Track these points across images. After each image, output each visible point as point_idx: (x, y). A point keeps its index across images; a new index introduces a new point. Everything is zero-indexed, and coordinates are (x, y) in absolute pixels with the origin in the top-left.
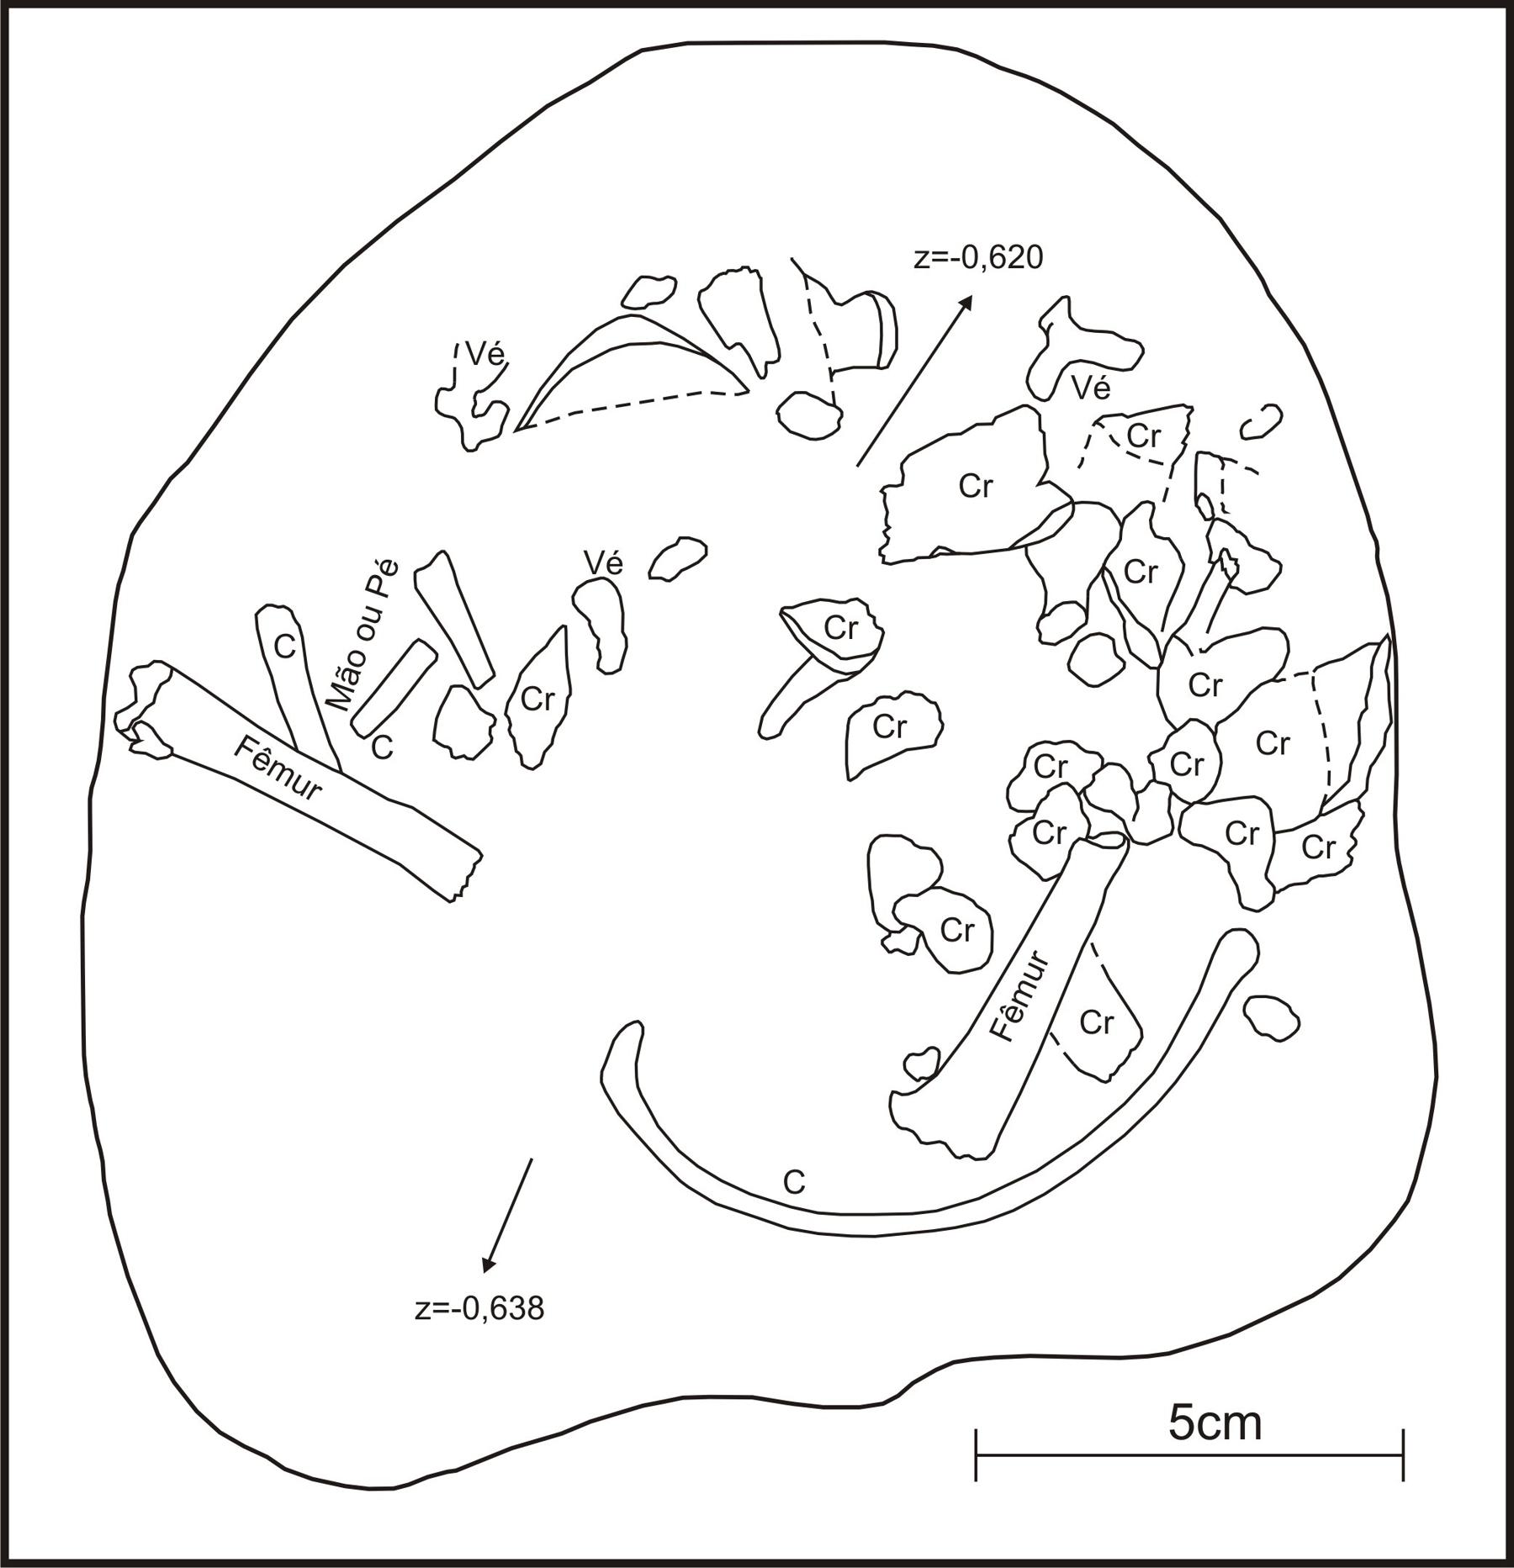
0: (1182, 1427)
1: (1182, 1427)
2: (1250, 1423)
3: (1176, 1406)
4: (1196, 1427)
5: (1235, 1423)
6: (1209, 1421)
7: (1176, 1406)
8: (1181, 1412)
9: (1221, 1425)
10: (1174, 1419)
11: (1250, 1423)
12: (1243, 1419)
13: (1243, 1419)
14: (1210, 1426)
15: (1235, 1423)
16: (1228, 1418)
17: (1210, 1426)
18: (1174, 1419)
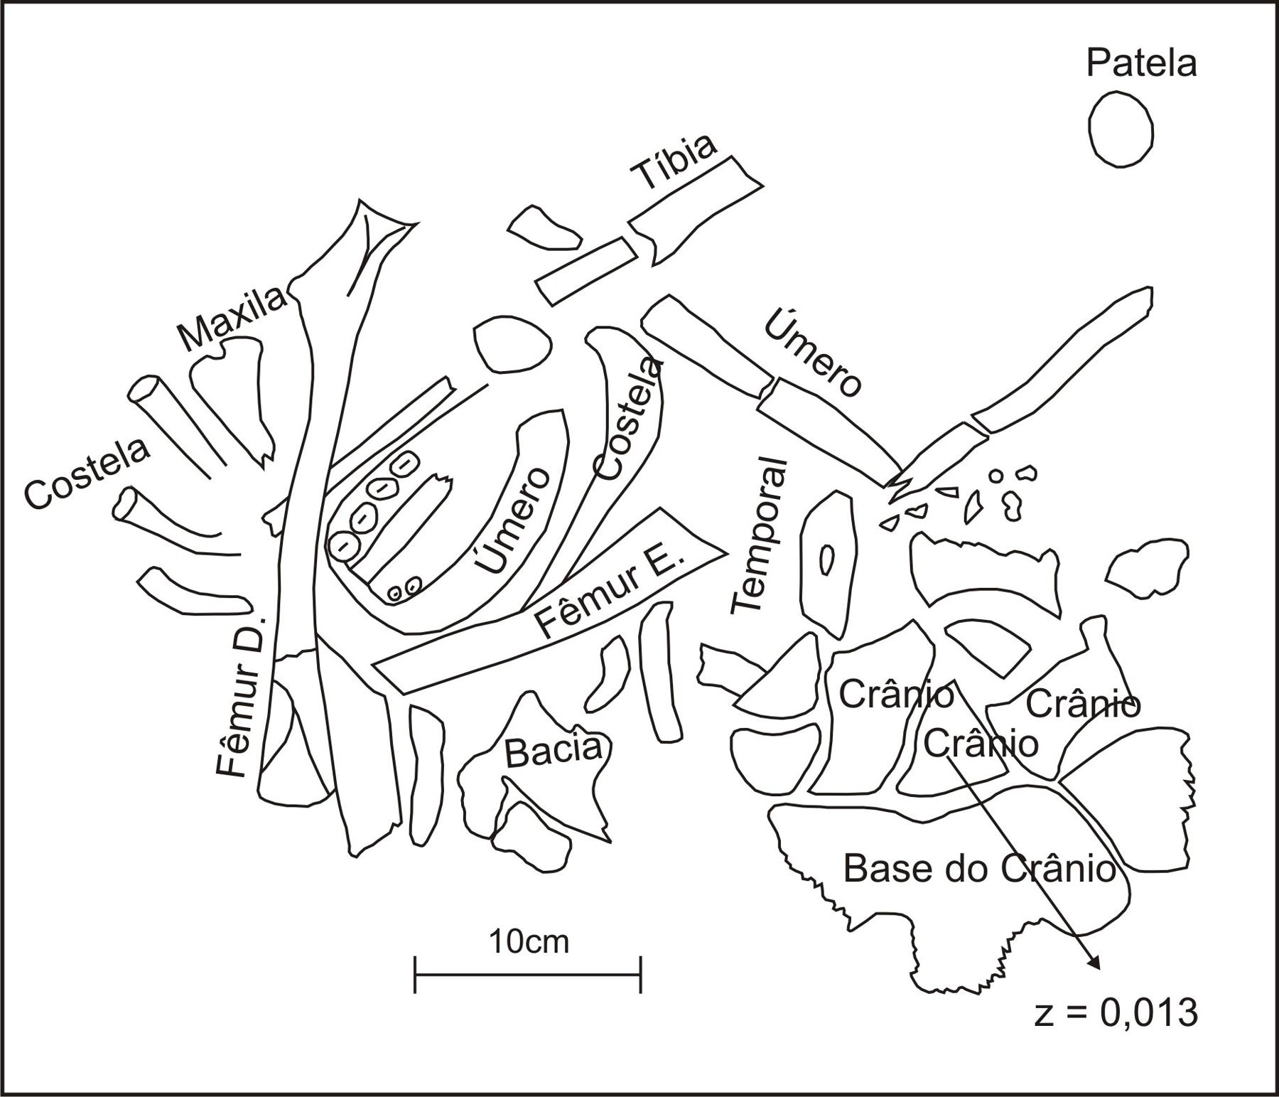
2: (561, 942)
4: (525, 943)
5: (551, 941)
6: (533, 940)
9: (541, 944)
11: (561, 942)
12: (556, 939)
13: (556, 939)
14: (534, 944)
15: (551, 941)
16: (546, 938)
17: (534, 944)
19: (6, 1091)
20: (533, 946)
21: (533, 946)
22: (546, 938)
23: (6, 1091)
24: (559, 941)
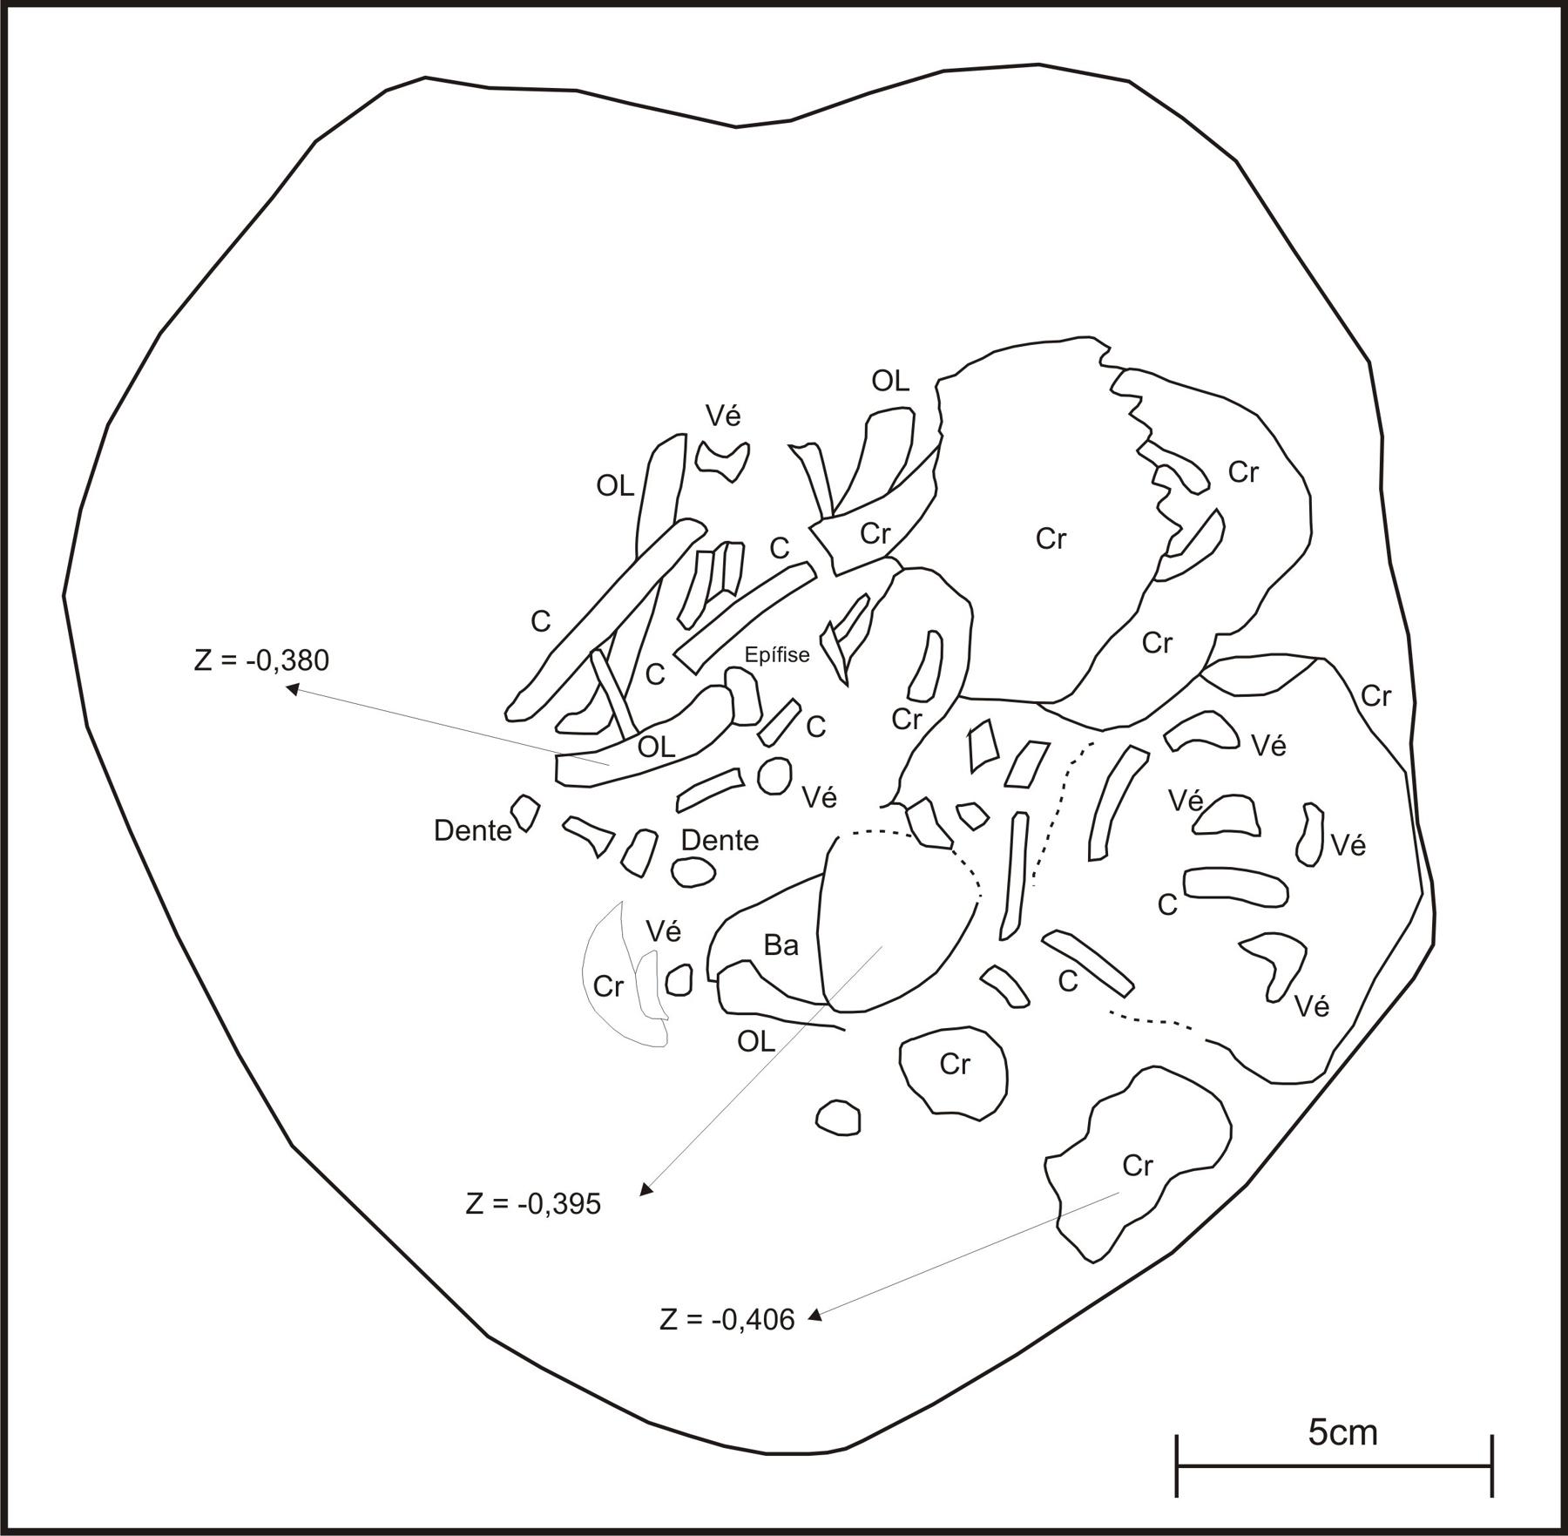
0: (1318, 1436)
1: (1318, 1436)
2: (1369, 1432)
3: (1314, 1420)
4: (1329, 1436)
5: (1358, 1432)
7: (1314, 1420)
8: (1317, 1424)
9: (1347, 1434)
10: (1312, 1430)
11: (1369, 1432)
12: (1363, 1430)
13: (1363, 1430)
15: (1358, 1432)
16: (1352, 1429)
17: (1340, 1435)
18: (1312, 1430)
19: (10, 1526)
20: (1338, 1439)
21: (1338, 1439)
22: (1352, 1429)
23: (10, 1526)
24: (1366, 1432)
